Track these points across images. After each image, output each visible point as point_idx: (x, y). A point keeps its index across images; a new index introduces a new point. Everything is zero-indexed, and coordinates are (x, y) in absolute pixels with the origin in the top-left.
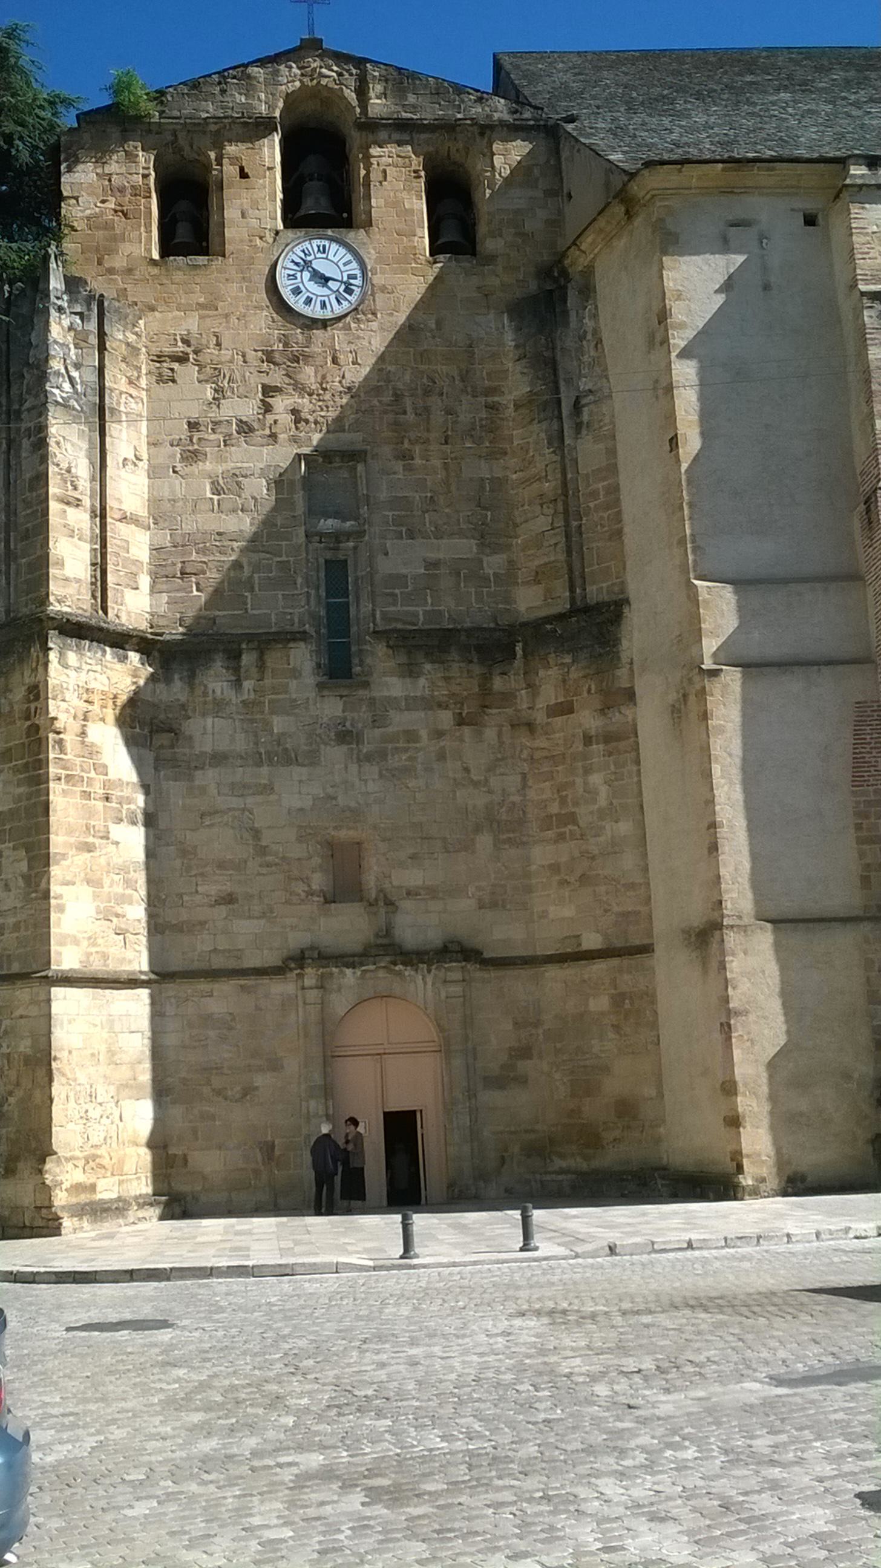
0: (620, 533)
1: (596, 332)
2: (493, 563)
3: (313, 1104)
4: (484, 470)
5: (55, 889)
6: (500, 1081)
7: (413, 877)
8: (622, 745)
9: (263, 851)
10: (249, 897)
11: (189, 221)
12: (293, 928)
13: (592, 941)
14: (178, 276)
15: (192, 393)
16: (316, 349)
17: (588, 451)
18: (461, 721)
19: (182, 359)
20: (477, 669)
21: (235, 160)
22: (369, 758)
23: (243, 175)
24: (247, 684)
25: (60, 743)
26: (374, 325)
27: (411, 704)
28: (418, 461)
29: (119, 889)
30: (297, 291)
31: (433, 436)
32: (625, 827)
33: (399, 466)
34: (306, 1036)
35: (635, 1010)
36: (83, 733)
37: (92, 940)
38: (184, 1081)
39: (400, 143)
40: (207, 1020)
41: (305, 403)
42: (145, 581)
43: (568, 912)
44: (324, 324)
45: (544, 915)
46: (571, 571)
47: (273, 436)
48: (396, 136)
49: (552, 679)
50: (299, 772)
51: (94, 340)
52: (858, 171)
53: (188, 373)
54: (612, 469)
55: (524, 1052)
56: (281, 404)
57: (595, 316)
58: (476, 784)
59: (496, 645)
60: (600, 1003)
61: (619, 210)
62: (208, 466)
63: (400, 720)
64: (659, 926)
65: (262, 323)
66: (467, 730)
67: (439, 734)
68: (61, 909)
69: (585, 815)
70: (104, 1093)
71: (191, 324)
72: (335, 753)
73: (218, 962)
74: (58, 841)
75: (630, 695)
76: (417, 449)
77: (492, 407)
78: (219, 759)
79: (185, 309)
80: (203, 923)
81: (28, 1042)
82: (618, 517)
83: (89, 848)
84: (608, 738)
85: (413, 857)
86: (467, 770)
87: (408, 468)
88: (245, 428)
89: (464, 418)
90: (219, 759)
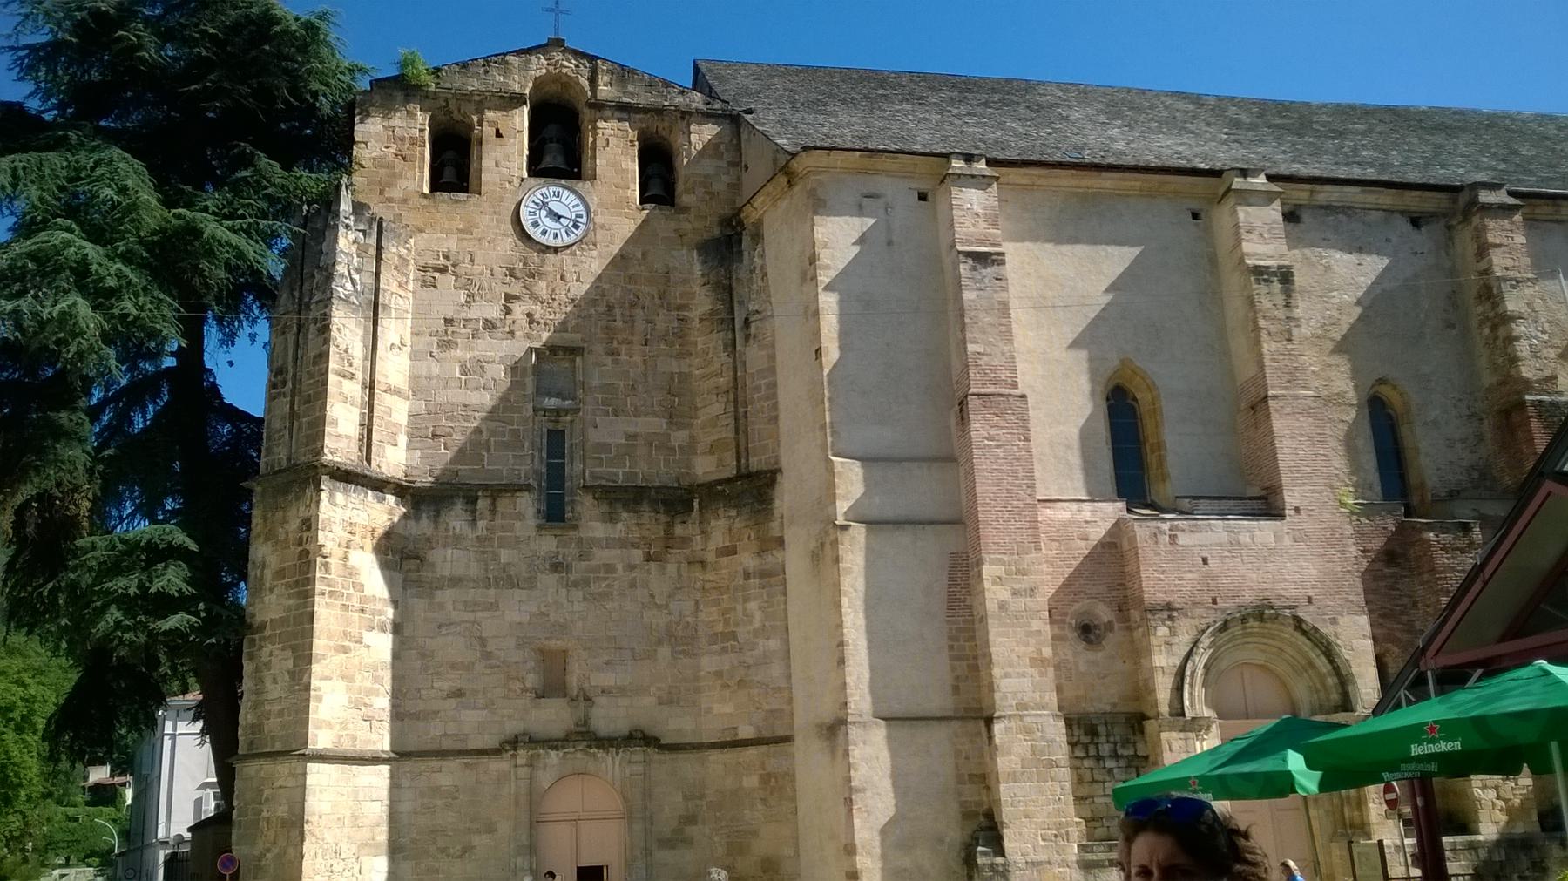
0: (776, 419)
1: (762, 267)
2: (679, 437)
3: (519, 860)
4: (674, 366)
5: (314, 683)
6: (668, 843)
7: (607, 679)
8: (773, 580)
9: (487, 655)
10: (475, 692)
11: (454, 164)
12: (510, 717)
13: (746, 732)
14: (443, 207)
15: (448, 296)
16: (548, 268)
17: (754, 356)
18: (649, 558)
19: (443, 270)
20: (663, 518)
21: (492, 123)
22: (575, 584)
23: (498, 135)
24: (481, 524)
25: (326, 565)
26: (595, 253)
27: (610, 543)
28: (623, 357)
29: (369, 684)
30: (536, 224)
31: (635, 339)
32: (774, 644)
33: (609, 360)
34: (517, 803)
35: (779, 786)
36: (346, 558)
37: (344, 725)
38: (414, 841)
39: (620, 120)
40: (435, 791)
41: (538, 310)
42: (403, 440)
43: (728, 709)
44: (556, 250)
45: (709, 710)
46: (738, 446)
47: (512, 333)
48: (617, 114)
49: (721, 527)
50: (518, 594)
51: (373, 252)
52: (958, 164)
53: (446, 281)
54: (772, 370)
55: (690, 819)
56: (519, 310)
57: (762, 256)
58: (659, 607)
59: (678, 501)
61: (783, 180)
62: (459, 353)
63: (602, 556)
64: (799, 721)
65: (508, 245)
66: (653, 565)
67: (632, 567)
68: (319, 699)
69: (743, 633)
70: (347, 850)
71: (452, 244)
72: (549, 580)
73: (447, 744)
74: (319, 644)
75: (781, 542)
76: (623, 347)
77: (682, 320)
78: (456, 582)
79: (449, 232)
80: (436, 713)
81: (286, 808)
82: (775, 406)
83: (345, 650)
84: (763, 574)
85: (608, 663)
86: (652, 596)
87: (616, 362)
88: (490, 325)
89: (661, 326)
90: (456, 582)
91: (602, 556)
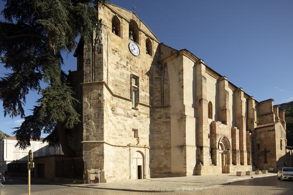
22: (138, 119)
52: (201, 61)
56: (129, 66)
60: (163, 154)
61: (176, 55)
62: (119, 70)
65: (127, 51)
88: (124, 67)
91: (142, 115)
